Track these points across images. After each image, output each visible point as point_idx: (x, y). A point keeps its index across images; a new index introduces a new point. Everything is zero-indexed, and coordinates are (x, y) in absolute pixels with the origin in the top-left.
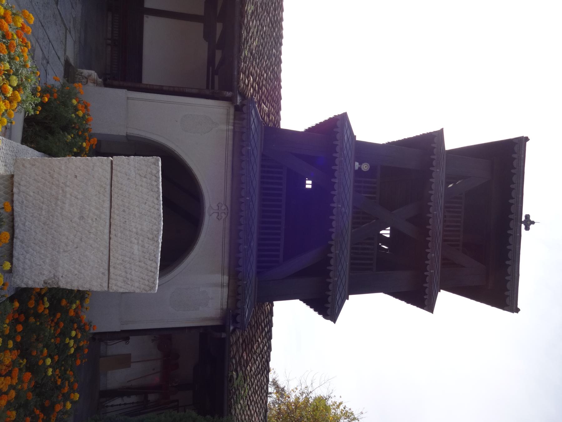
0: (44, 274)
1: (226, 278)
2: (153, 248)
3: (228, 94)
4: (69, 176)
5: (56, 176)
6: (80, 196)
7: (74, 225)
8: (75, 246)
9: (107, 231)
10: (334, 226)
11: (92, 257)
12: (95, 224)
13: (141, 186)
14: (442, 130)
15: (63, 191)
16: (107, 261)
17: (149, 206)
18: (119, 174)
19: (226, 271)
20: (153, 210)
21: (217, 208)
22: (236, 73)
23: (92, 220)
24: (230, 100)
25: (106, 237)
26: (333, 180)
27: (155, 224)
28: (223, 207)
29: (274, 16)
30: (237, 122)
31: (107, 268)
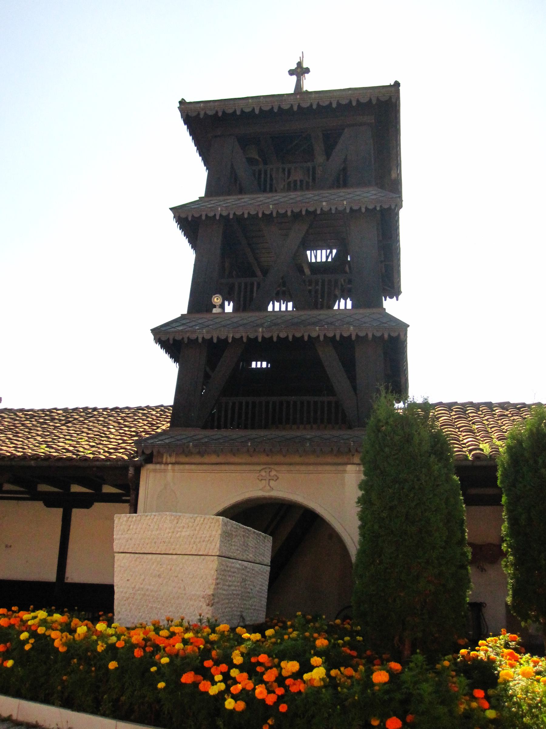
0: (201, 606)
1: (349, 468)
2: (184, 520)
3: (131, 471)
4: (128, 585)
5: (127, 595)
6: (143, 577)
7: (164, 582)
8: (181, 581)
9: (170, 556)
10: (285, 335)
11: (190, 568)
12: (165, 566)
13: (136, 529)
14: (171, 209)
15: (138, 590)
16: (194, 557)
17: (152, 522)
18: (127, 547)
19: (340, 468)
20: (155, 520)
21: (263, 482)
22: (108, 463)
23: (161, 568)
24: (138, 470)
25: (175, 557)
26: (230, 340)
27: (166, 518)
28: (263, 473)
29: (60, 420)
30: (164, 460)
31: (199, 557)
